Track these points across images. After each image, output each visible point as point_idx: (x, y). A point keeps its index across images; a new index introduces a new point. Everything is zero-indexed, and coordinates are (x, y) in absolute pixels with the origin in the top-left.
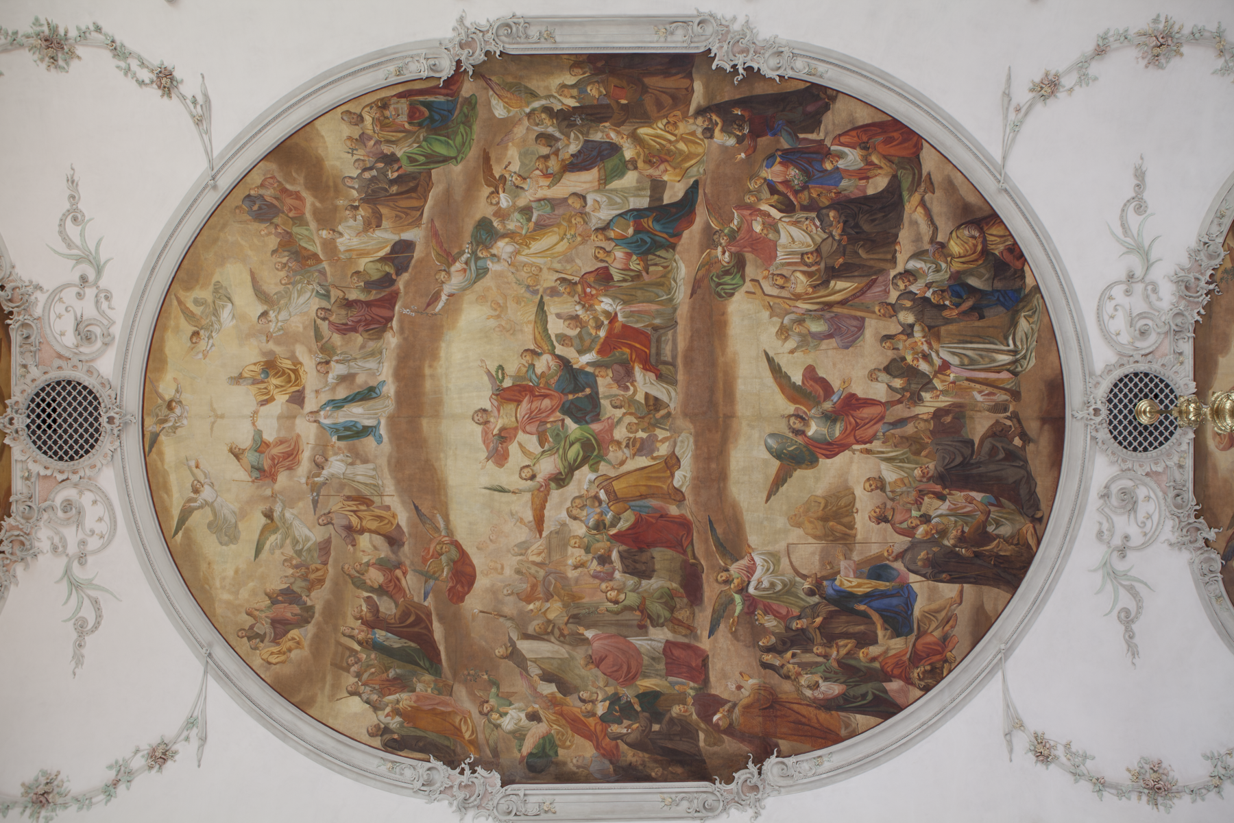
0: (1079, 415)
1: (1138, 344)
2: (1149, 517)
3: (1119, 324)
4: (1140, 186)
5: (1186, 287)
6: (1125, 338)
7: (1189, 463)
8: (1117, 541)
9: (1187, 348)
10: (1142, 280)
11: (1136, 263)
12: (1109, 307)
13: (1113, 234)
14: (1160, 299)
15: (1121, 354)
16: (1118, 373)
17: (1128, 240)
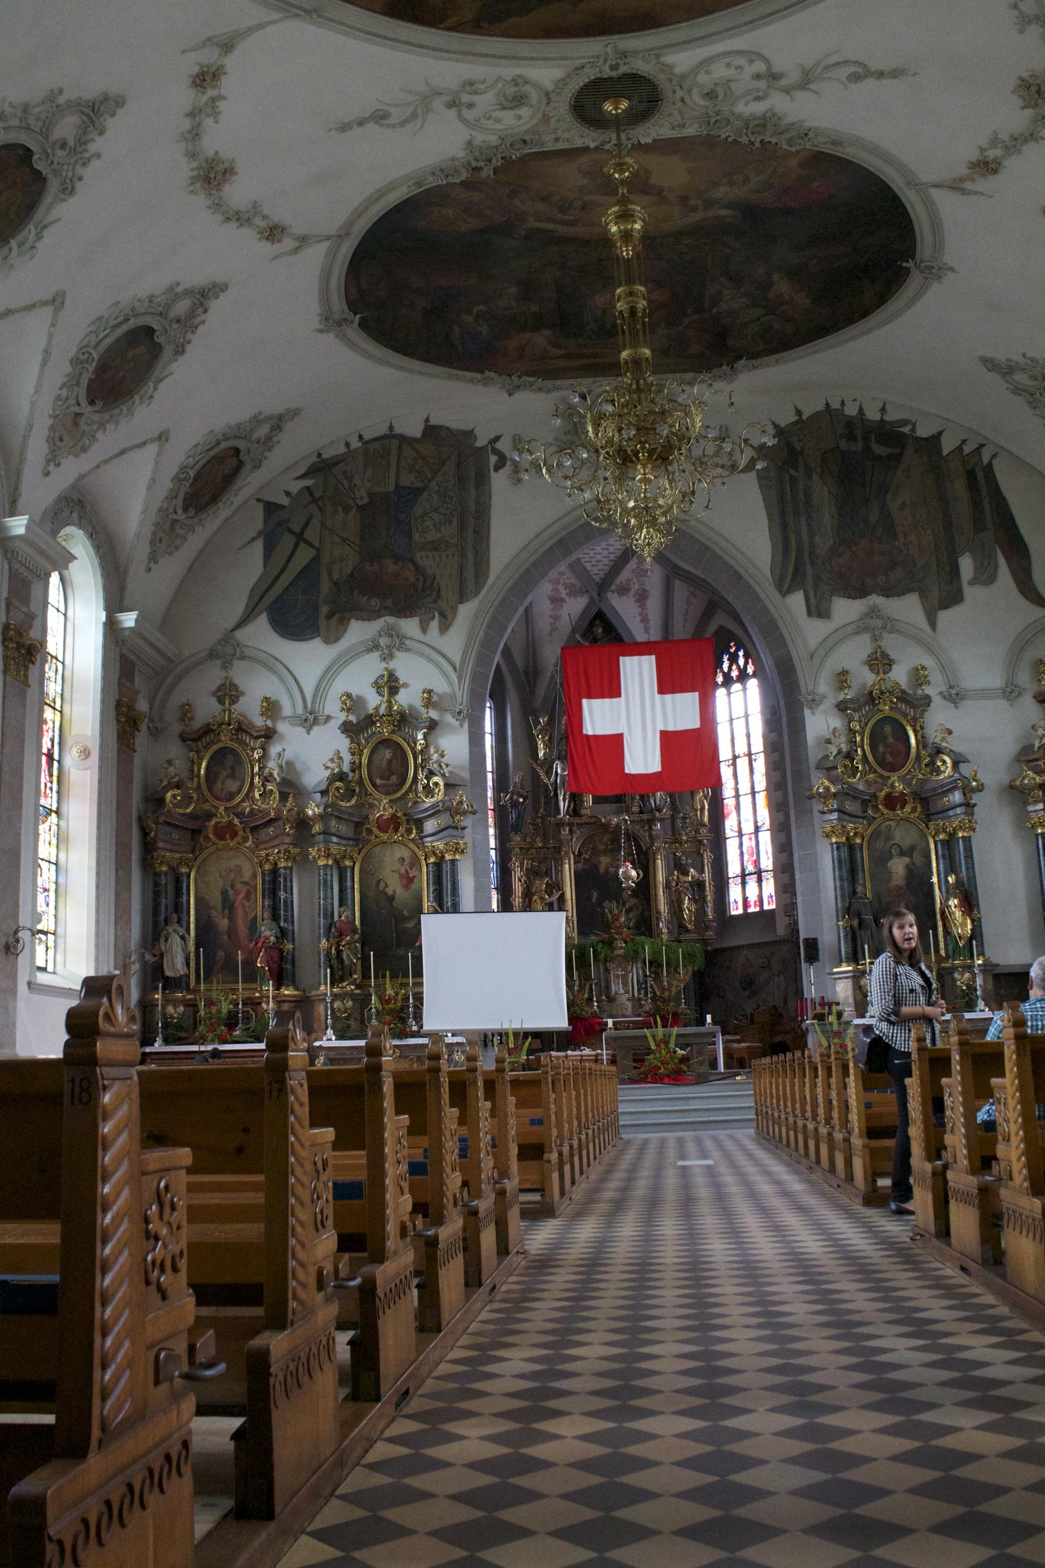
0: (609, 50)
1: (695, 91)
2: (498, 121)
3: (720, 71)
4: (881, 75)
5: (763, 122)
6: (702, 78)
7: (561, 146)
8: (465, 98)
9: (690, 131)
10: (769, 87)
11: (793, 77)
12: (742, 61)
13: (829, 55)
14: (746, 104)
15: (683, 77)
16: (661, 79)
17: (820, 69)
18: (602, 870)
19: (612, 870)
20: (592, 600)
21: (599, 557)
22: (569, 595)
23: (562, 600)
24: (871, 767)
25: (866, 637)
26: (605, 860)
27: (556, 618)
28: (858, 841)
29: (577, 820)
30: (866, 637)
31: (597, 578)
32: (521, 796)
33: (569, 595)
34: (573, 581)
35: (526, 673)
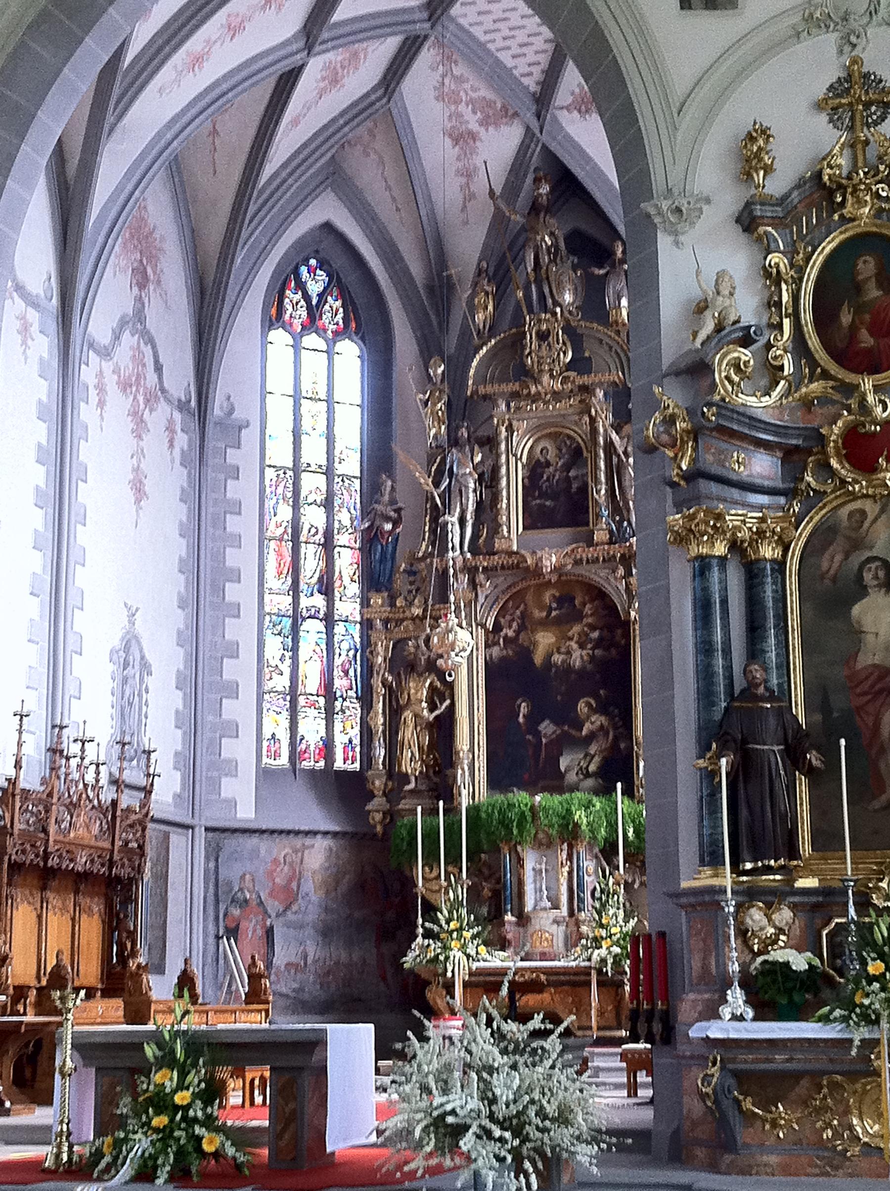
18: (538, 658)
19: (557, 658)
20: (528, 129)
21: (521, 36)
22: (485, 122)
23: (473, 136)
24: (813, 363)
25: (830, 40)
26: (545, 640)
27: (468, 174)
28: (768, 551)
29: (483, 562)
30: (830, 40)
31: (534, 88)
32: (388, 519)
33: (485, 122)
34: (485, 92)
35: (430, 289)
